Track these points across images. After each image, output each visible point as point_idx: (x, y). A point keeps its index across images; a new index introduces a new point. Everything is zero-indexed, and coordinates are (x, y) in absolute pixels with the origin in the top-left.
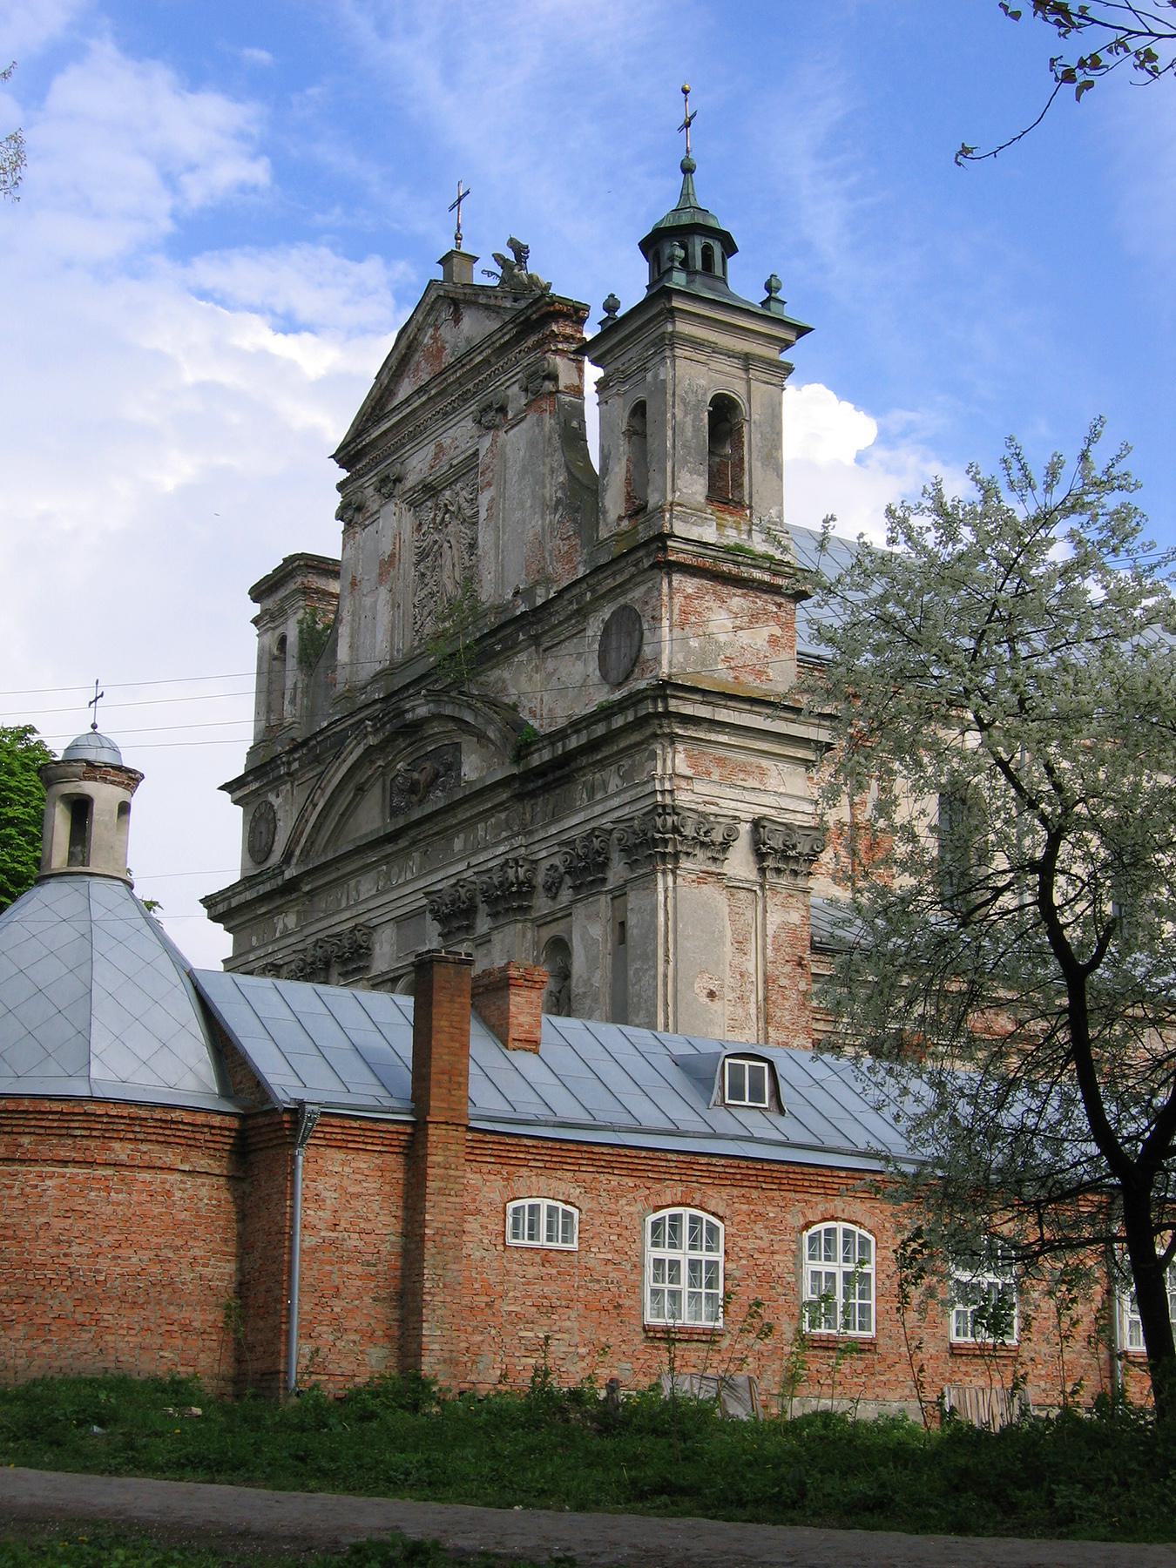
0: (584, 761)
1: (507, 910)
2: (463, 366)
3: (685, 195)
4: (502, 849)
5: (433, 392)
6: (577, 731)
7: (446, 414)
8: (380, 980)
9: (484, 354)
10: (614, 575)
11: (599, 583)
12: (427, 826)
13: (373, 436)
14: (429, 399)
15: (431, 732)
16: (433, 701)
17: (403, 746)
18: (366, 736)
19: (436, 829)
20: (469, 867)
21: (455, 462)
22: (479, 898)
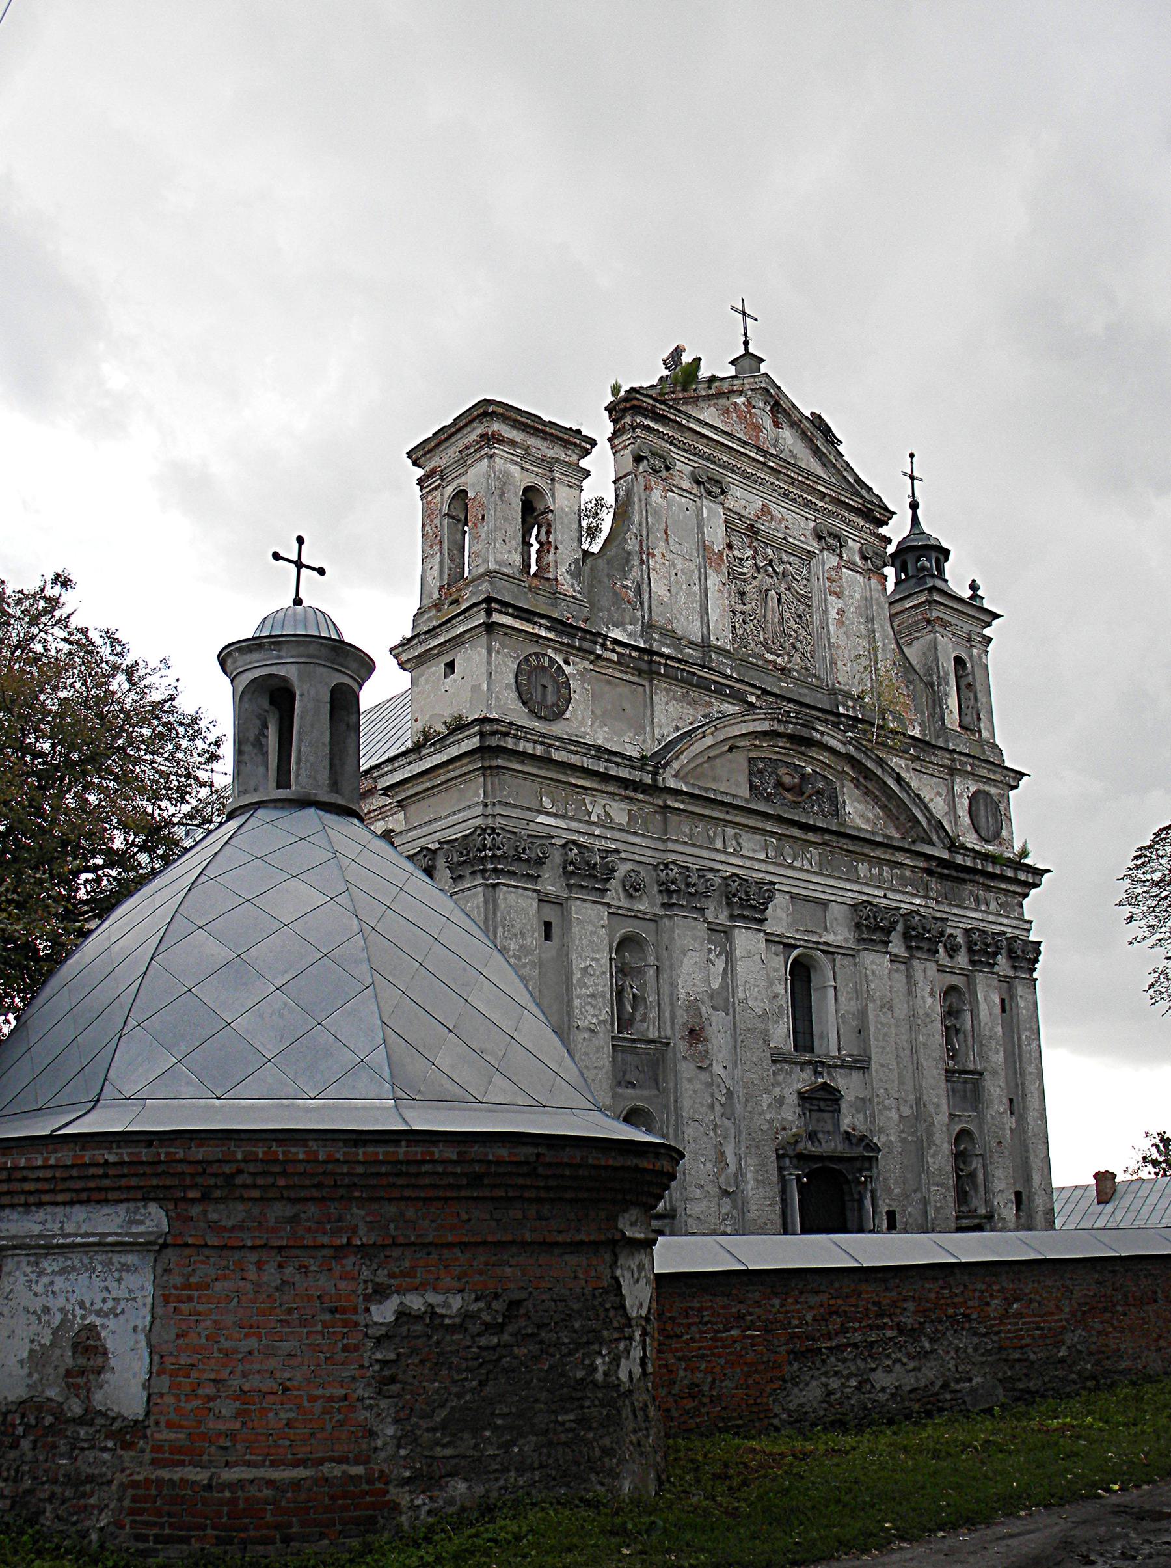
0: (981, 880)
1: (929, 950)
2: (807, 478)
3: (915, 520)
4: (917, 901)
5: (772, 464)
6: (994, 863)
7: (786, 495)
8: (777, 939)
9: (829, 491)
10: (989, 771)
11: (979, 767)
12: (845, 841)
13: (691, 425)
14: (764, 464)
15: (815, 755)
16: (854, 746)
17: (780, 744)
18: (773, 719)
19: (851, 848)
20: (885, 896)
21: (791, 540)
22: (900, 927)
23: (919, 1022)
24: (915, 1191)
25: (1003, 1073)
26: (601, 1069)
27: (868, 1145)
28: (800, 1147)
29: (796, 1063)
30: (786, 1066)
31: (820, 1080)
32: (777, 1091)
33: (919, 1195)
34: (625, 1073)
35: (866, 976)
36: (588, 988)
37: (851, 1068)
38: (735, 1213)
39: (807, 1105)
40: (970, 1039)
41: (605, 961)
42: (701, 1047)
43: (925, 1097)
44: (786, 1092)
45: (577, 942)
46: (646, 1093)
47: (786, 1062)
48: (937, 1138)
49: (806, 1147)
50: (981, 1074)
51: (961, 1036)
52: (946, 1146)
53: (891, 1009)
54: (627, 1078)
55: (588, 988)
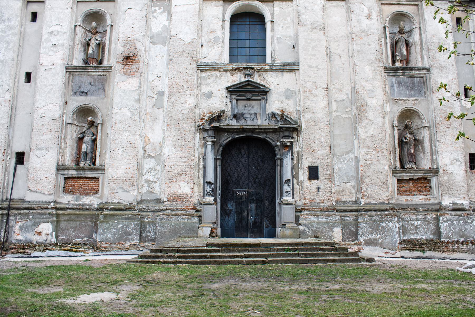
23: (354, 36)
24: (347, 153)
25: (455, 68)
26: (55, 85)
27: (286, 119)
28: (223, 124)
29: (226, 71)
30: (218, 73)
31: (247, 79)
32: (205, 89)
33: (352, 156)
34: (80, 87)
35: (298, 12)
36: (52, 42)
37: (282, 70)
38: (158, 167)
39: (233, 97)
40: (418, 48)
41: (67, 26)
42: (133, 66)
43: (357, 87)
44: (215, 90)
45: (48, 19)
46: (93, 98)
47: (215, 70)
48: (370, 115)
49: (234, 124)
50: (428, 70)
51: (413, 49)
52: (380, 120)
53: (323, 29)
54: (82, 90)
55: (52, 42)
